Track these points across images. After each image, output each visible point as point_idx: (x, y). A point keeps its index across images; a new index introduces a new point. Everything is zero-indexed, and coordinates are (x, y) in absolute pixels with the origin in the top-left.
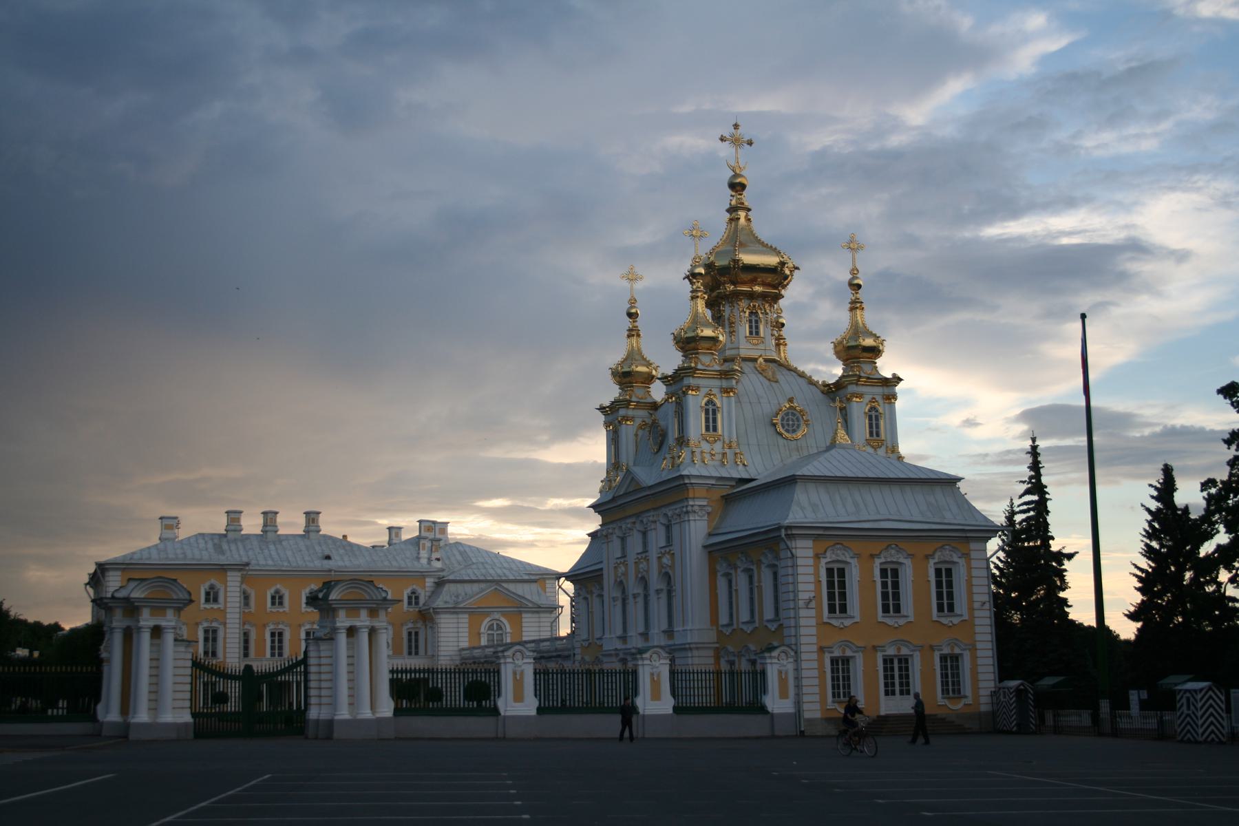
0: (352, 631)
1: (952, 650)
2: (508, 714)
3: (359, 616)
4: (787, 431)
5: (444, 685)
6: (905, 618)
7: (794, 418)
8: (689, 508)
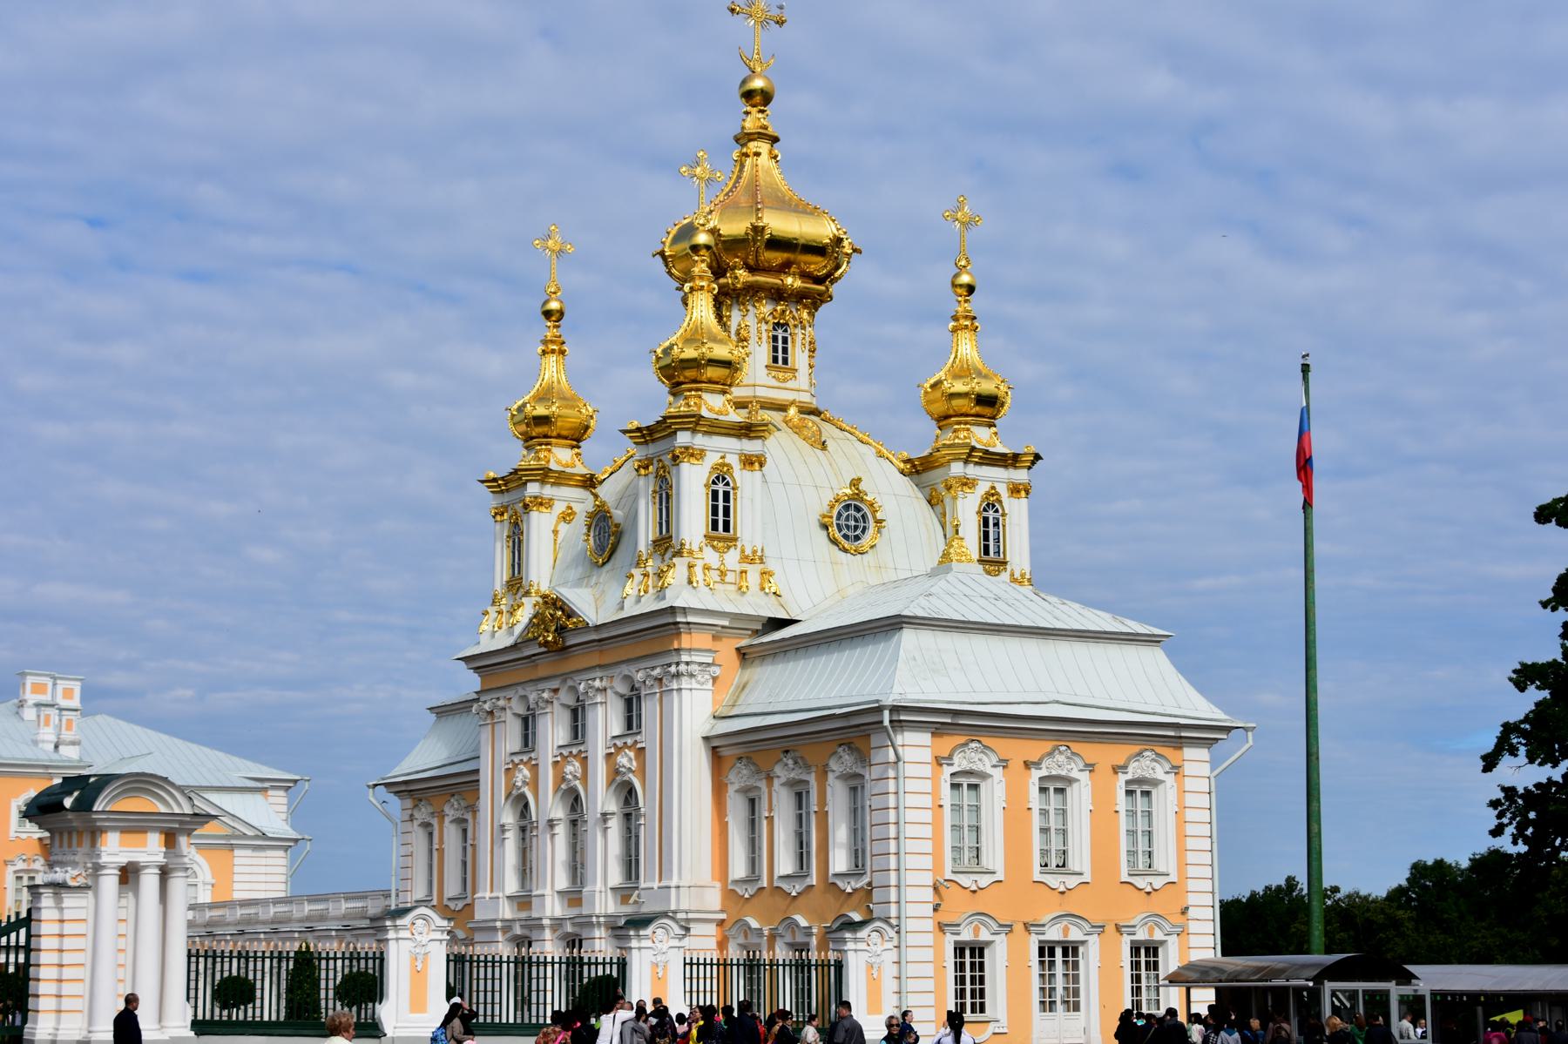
0: (129, 875)
1: (1066, 934)
3: (145, 845)
4: (846, 537)
6: (991, 875)
7: (859, 515)
8: (682, 668)
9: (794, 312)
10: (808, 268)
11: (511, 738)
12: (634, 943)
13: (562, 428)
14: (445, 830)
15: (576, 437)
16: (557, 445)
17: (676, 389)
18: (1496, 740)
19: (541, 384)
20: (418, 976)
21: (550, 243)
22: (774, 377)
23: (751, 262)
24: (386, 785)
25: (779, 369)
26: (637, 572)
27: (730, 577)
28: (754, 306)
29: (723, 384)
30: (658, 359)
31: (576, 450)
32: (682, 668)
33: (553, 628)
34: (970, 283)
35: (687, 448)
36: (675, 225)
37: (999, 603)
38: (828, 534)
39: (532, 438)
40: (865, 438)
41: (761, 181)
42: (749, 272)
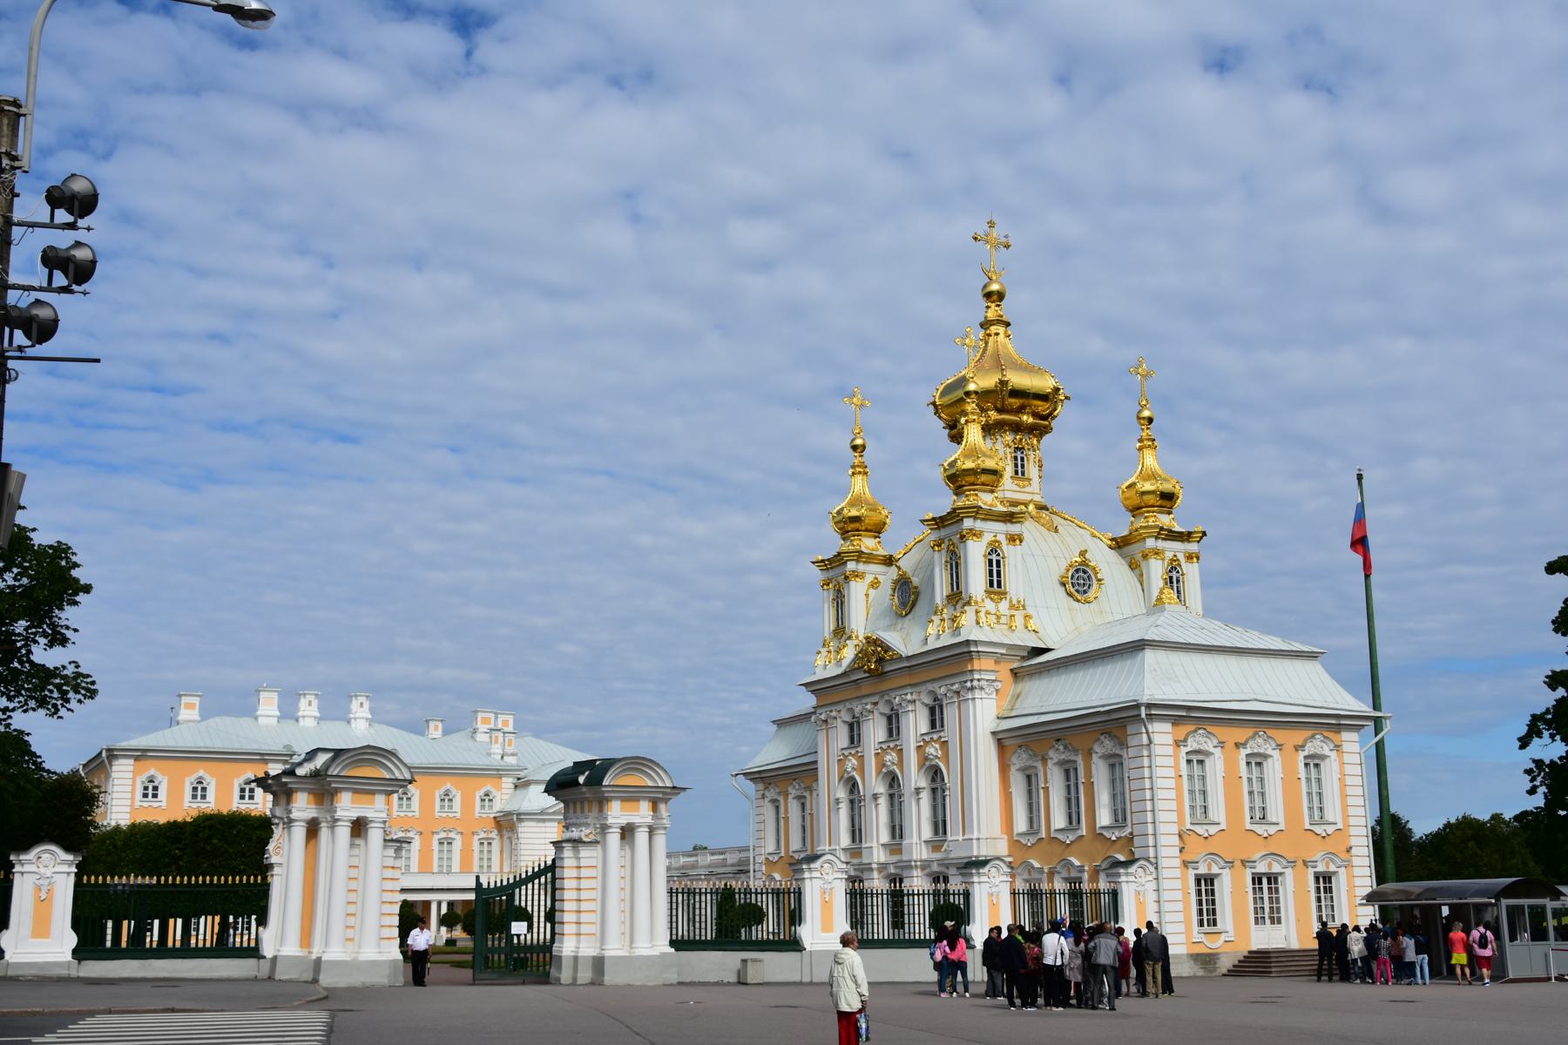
0: (627, 832)
2: (815, 948)
3: (638, 810)
4: (1077, 591)
5: (536, 908)
7: (1085, 576)
8: (975, 683)
11: (841, 737)
12: (975, 879)
13: (868, 525)
14: (789, 805)
15: (877, 530)
16: (865, 536)
17: (958, 491)
18: (1527, 728)
20: (827, 905)
21: (855, 400)
23: (999, 406)
24: (744, 774)
25: (1019, 479)
26: (936, 619)
27: (1003, 620)
29: (992, 486)
30: (945, 470)
31: (878, 539)
32: (975, 683)
33: (874, 660)
35: (971, 530)
37: (1204, 631)
38: (1066, 590)
39: (848, 532)
40: (1082, 525)
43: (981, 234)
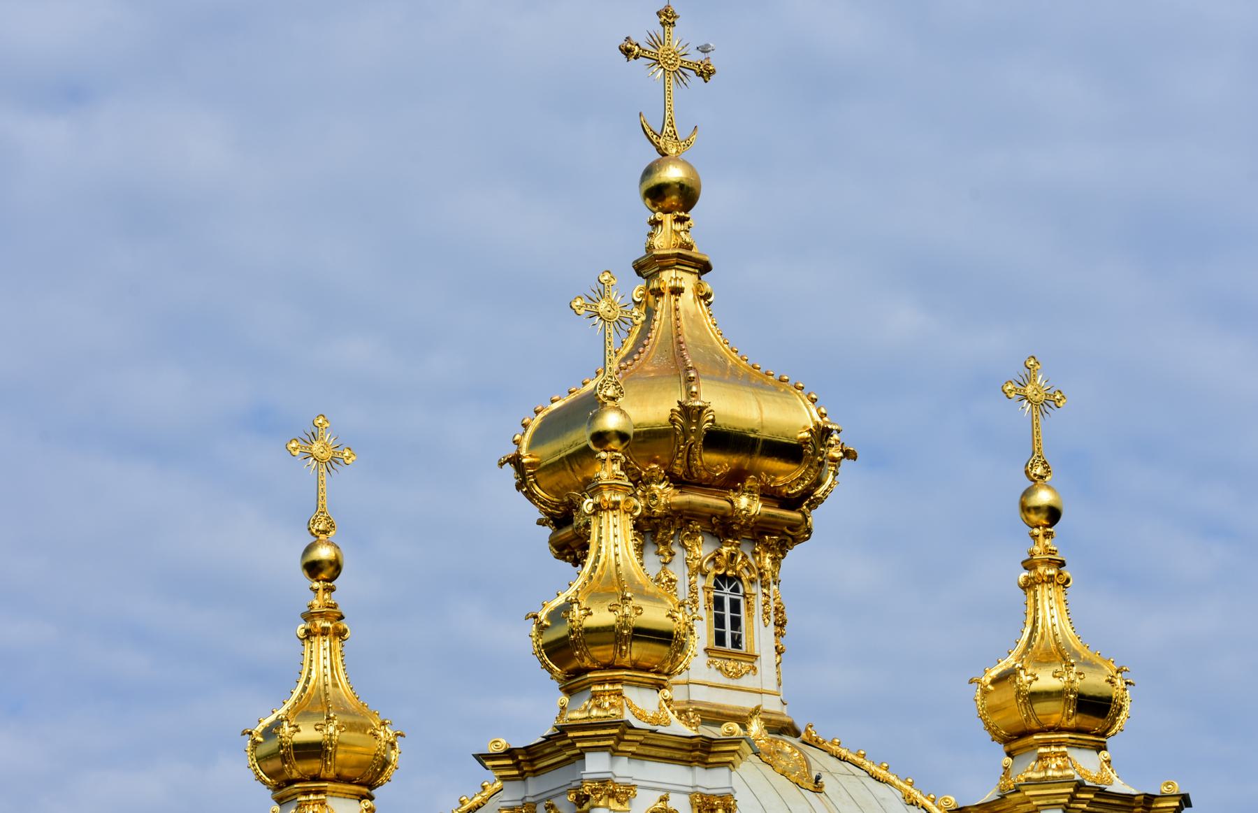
9: (750, 559)
10: (773, 480)
13: (343, 766)
16: (335, 794)
17: (573, 683)
19: (304, 689)
21: (316, 447)
22: (720, 669)
23: (679, 470)
25: (727, 656)
28: (683, 546)
29: (658, 672)
30: (542, 629)
31: (368, 803)
34: (1053, 504)
35: (604, 782)
36: (537, 412)
39: (290, 782)
40: (882, 773)
41: (686, 336)
42: (675, 488)
43: (641, 38)
